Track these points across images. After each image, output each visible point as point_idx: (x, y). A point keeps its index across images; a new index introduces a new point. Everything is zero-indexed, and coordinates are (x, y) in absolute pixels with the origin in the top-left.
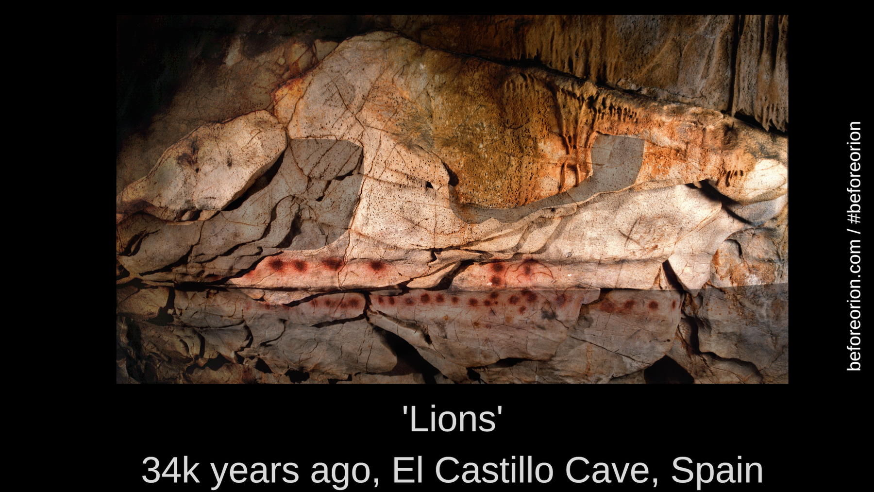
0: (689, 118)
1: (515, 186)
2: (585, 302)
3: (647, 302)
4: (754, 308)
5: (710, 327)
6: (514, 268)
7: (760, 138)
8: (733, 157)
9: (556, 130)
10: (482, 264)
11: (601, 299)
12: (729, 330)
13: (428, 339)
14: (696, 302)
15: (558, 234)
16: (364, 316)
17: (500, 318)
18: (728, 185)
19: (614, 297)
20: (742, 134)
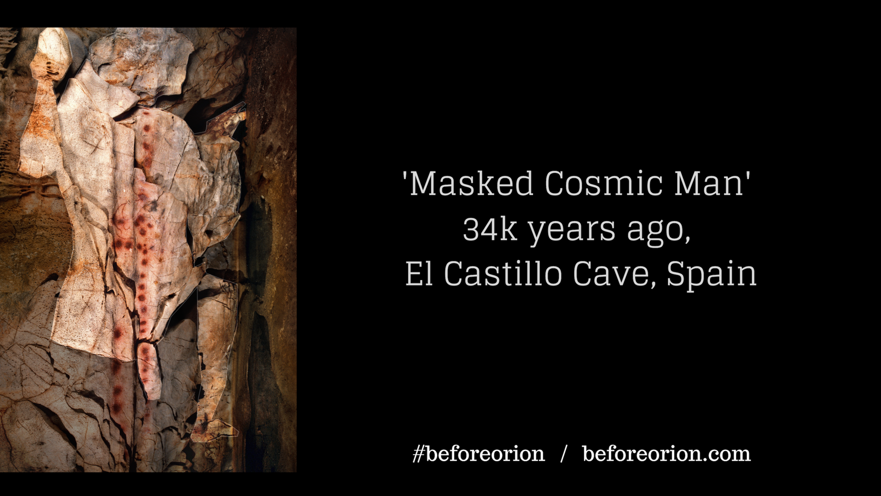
0: (8, 103)
1: (59, 232)
2: (144, 179)
3: (144, 133)
4: (148, 54)
5: (163, 87)
6: (119, 232)
7: (23, 48)
8: (37, 69)
9: (17, 201)
10: (116, 256)
11: (142, 168)
12: (165, 72)
13: (171, 296)
14: (144, 97)
15: (93, 199)
16: (154, 343)
17: (156, 242)
18: (57, 74)
19: (140, 157)
20: (19, 63)
